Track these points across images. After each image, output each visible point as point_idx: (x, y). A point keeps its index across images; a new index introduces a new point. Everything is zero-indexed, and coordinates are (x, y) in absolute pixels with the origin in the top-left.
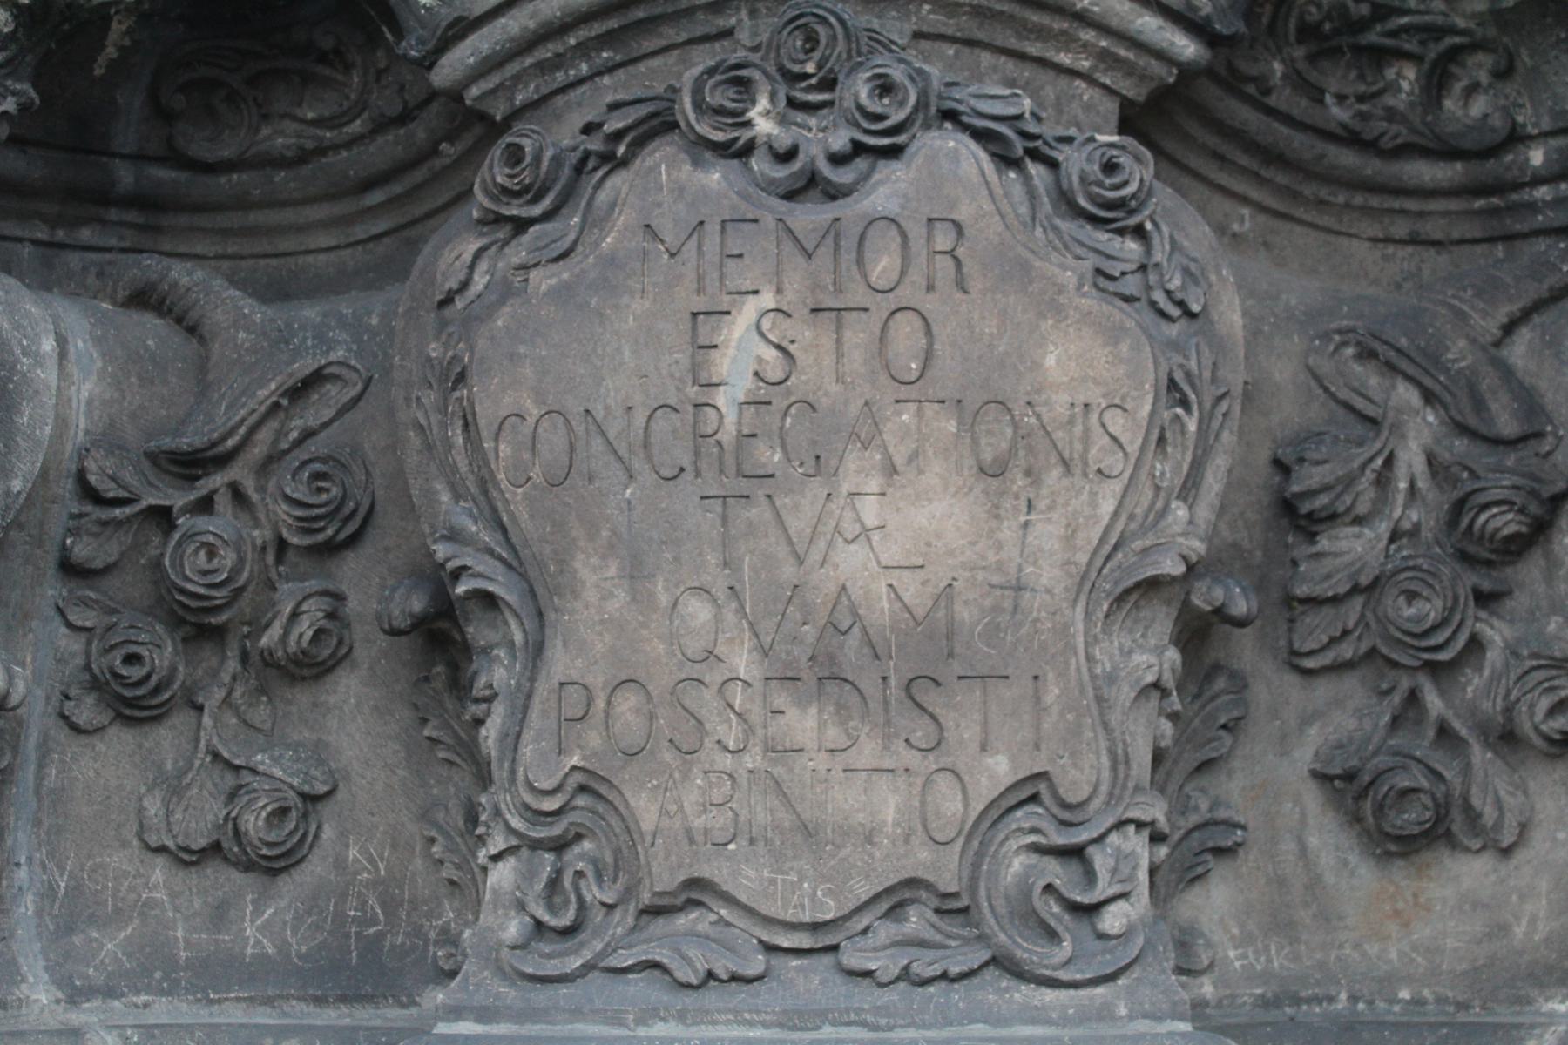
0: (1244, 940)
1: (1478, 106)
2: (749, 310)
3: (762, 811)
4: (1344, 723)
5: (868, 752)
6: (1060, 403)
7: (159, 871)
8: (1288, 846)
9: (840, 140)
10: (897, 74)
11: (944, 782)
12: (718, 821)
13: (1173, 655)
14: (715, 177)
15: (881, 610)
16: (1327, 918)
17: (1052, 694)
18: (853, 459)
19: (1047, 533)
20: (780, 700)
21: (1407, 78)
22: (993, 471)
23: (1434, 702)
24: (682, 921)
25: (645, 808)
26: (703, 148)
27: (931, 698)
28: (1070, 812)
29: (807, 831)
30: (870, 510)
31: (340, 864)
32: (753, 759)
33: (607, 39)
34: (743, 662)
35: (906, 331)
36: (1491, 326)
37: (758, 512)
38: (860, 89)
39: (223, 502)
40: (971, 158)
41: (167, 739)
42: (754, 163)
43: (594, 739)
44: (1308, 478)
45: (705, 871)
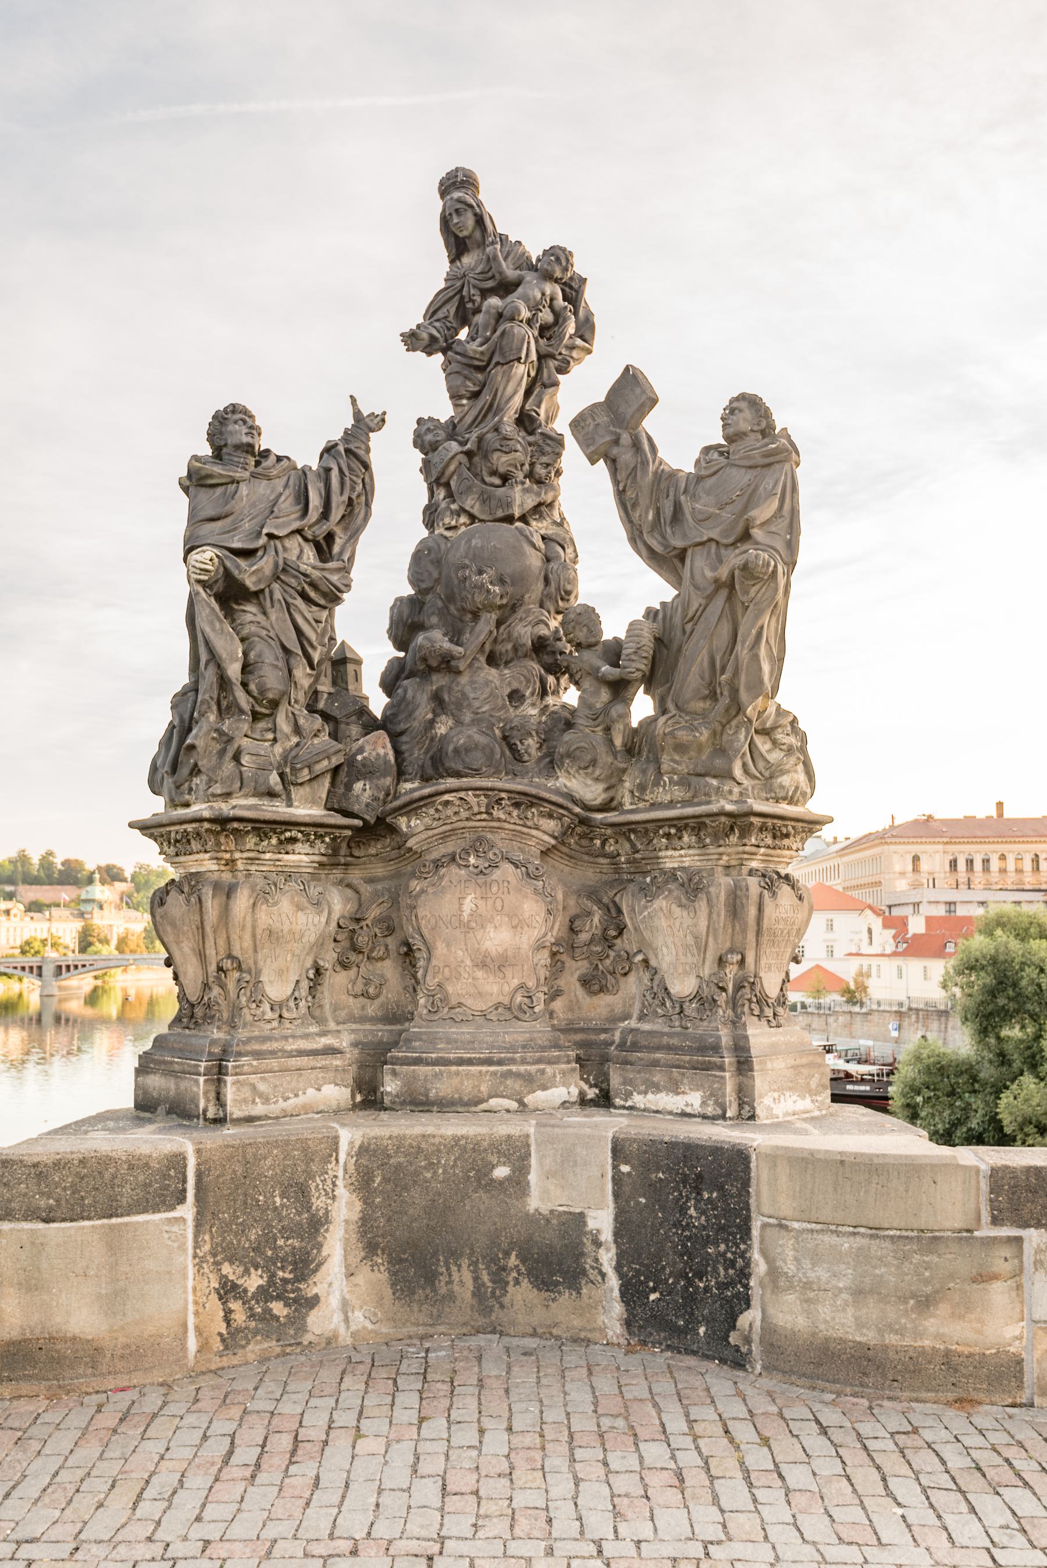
0: (564, 1012)
1: (612, 848)
2: (469, 898)
3: (472, 990)
4: (584, 970)
5: (491, 979)
6: (527, 915)
7: (351, 999)
8: (573, 994)
9: (486, 865)
10: (497, 852)
11: (506, 985)
12: (464, 992)
13: (549, 960)
14: (463, 872)
15: (494, 953)
16: (580, 1008)
17: (525, 968)
18: (489, 925)
19: (525, 938)
20: (475, 969)
21: (598, 842)
22: (515, 927)
23: (600, 966)
24: (457, 1010)
25: (450, 989)
26: (459, 866)
27: (503, 969)
28: (528, 990)
29: (479, 993)
30: (492, 934)
31: (387, 998)
32: (470, 980)
33: (441, 838)
34: (468, 962)
35: (499, 902)
36: (612, 894)
37: (471, 935)
38: (491, 855)
39: (365, 928)
40: (510, 867)
41: (353, 972)
42: (471, 868)
43: (440, 976)
44: (577, 923)
45: (462, 1001)
